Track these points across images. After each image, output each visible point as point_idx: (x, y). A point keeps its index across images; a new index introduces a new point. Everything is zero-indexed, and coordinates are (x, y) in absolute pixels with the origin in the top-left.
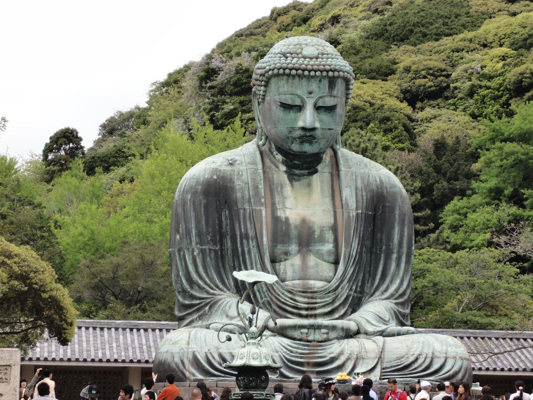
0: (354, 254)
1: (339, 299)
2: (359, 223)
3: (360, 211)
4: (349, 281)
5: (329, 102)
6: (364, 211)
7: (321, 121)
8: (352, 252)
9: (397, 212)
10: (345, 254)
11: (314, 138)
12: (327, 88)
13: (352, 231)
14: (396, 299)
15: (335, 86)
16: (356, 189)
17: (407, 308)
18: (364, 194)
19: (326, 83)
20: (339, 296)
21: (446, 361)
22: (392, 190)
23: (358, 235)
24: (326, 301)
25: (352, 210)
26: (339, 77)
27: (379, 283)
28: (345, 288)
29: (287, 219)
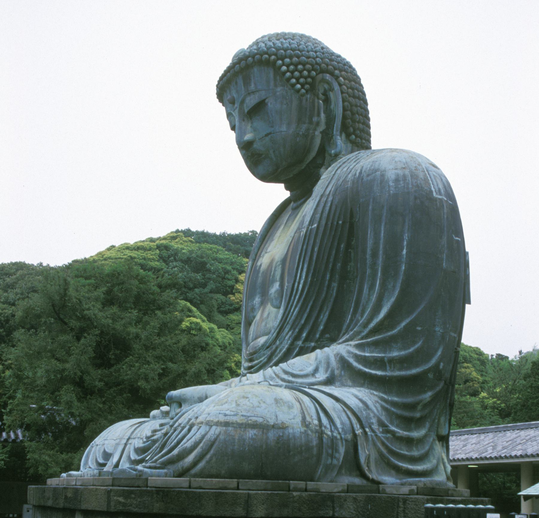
0: (301, 286)
1: (277, 356)
2: (312, 242)
3: (315, 225)
4: (293, 327)
5: (251, 101)
6: (323, 222)
7: (255, 130)
8: (296, 285)
9: (370, 207)
10: (287, 290)
11: (260, 155)
12: (243, 87)
13: (298, 256)
14: (362, 338)
15: (250, 79)
16: (322, 196)
17: (404, 348)
18: (330, 199)
19: (240, 81)
20: (278, 351)
21: (189, 430)
22: (369, 178)
23: (307, 259)
24: (261, 362)
25: (304, 227)
26: (248, 67)
27: (352, 320)
28: (287, 338)
29: (261, 265)
